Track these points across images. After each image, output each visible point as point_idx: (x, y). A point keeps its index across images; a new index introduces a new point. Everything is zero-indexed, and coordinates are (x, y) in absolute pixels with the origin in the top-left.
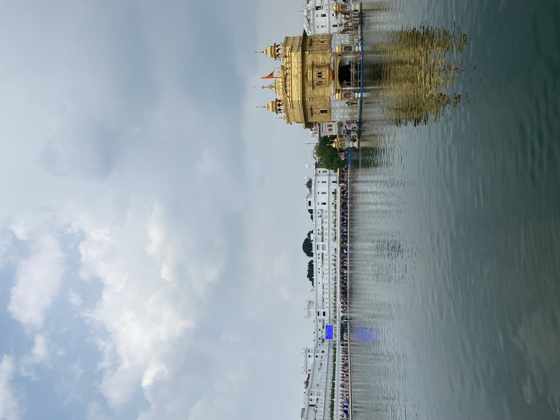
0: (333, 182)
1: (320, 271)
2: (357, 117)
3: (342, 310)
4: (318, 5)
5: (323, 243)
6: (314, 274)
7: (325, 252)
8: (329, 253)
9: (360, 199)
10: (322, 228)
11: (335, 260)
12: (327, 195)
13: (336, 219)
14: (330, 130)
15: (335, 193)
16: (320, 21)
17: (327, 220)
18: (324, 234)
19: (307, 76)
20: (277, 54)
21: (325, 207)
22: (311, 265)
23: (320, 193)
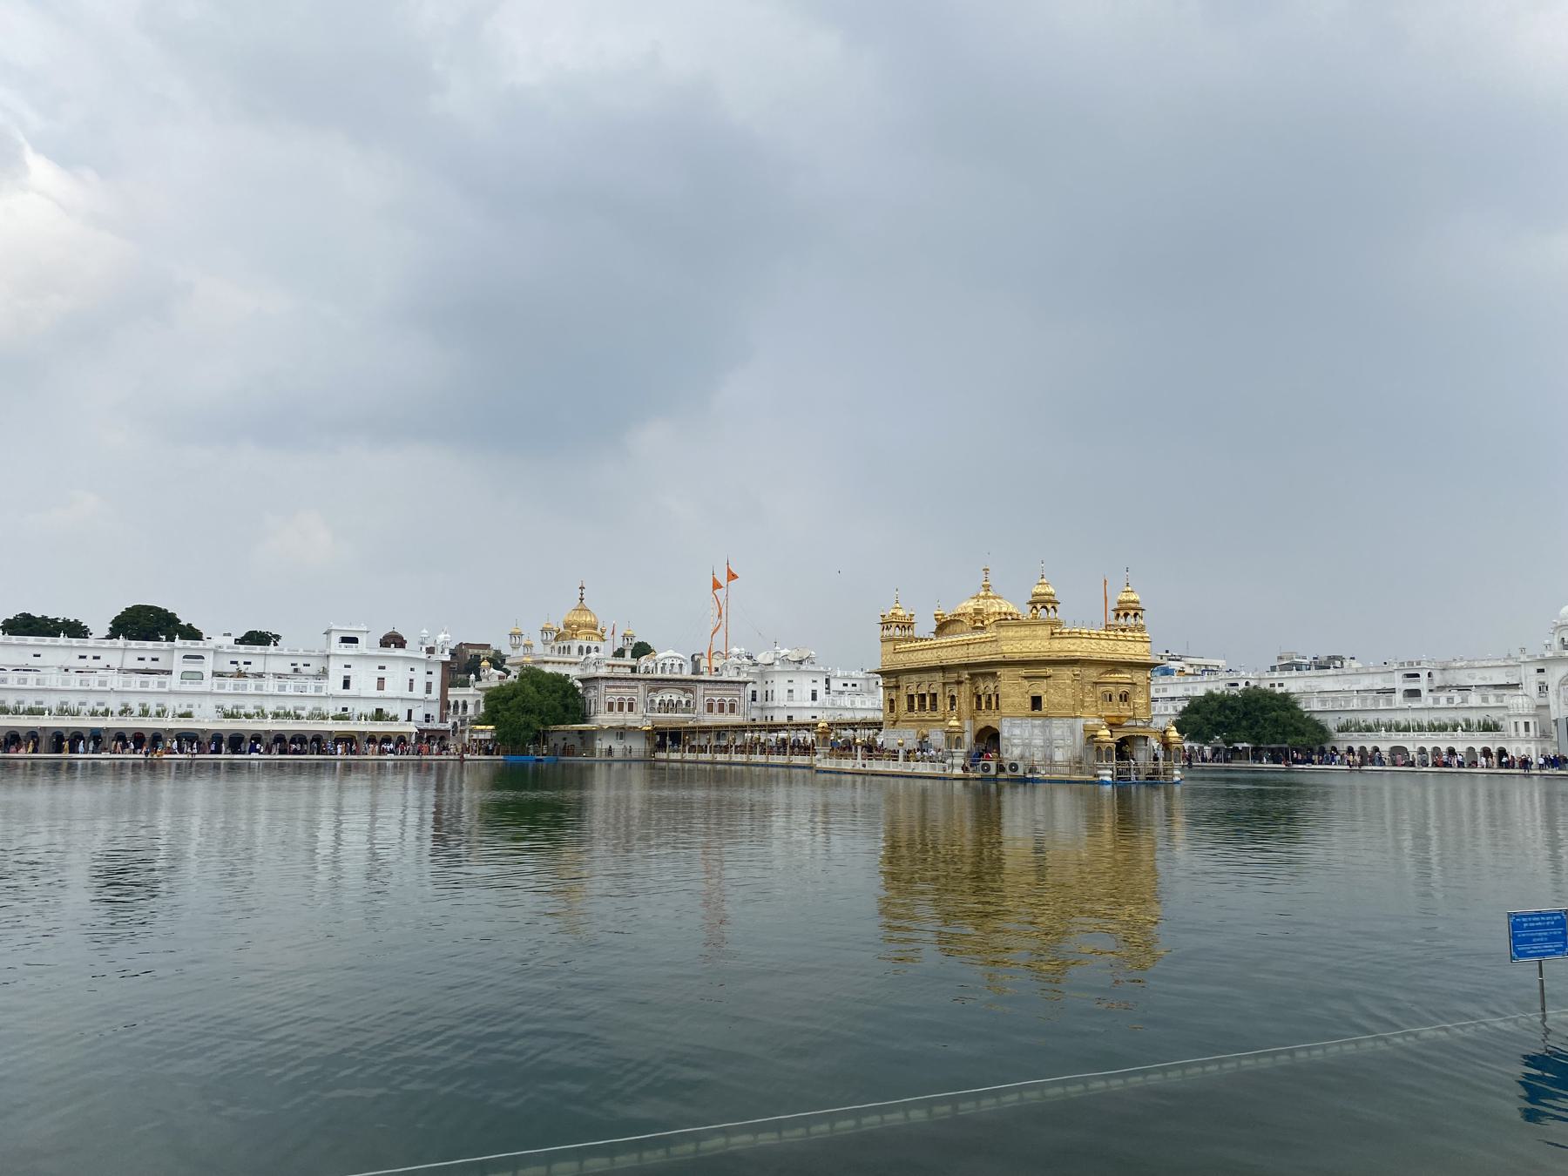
0: (410, 712)
1: (89, 662)
2: (1042, 773)
3: (1429, 749)
4: (832, 682)
5: (208, 674)
6: (74, 641)
7: (174, 682)
8: (171, 692)
9: (357, 792)
10: (260, 675)
11: (145, 713)
12: (375, 693)
13: (298, 717)
14: (611, 707)
15: (379, 715)
16: (804, 686)
17: (289, 691)
18: (241, 681)
19: (1115, 671)
21: (334, 685)
22: (76, 630)
23: (381, 674)
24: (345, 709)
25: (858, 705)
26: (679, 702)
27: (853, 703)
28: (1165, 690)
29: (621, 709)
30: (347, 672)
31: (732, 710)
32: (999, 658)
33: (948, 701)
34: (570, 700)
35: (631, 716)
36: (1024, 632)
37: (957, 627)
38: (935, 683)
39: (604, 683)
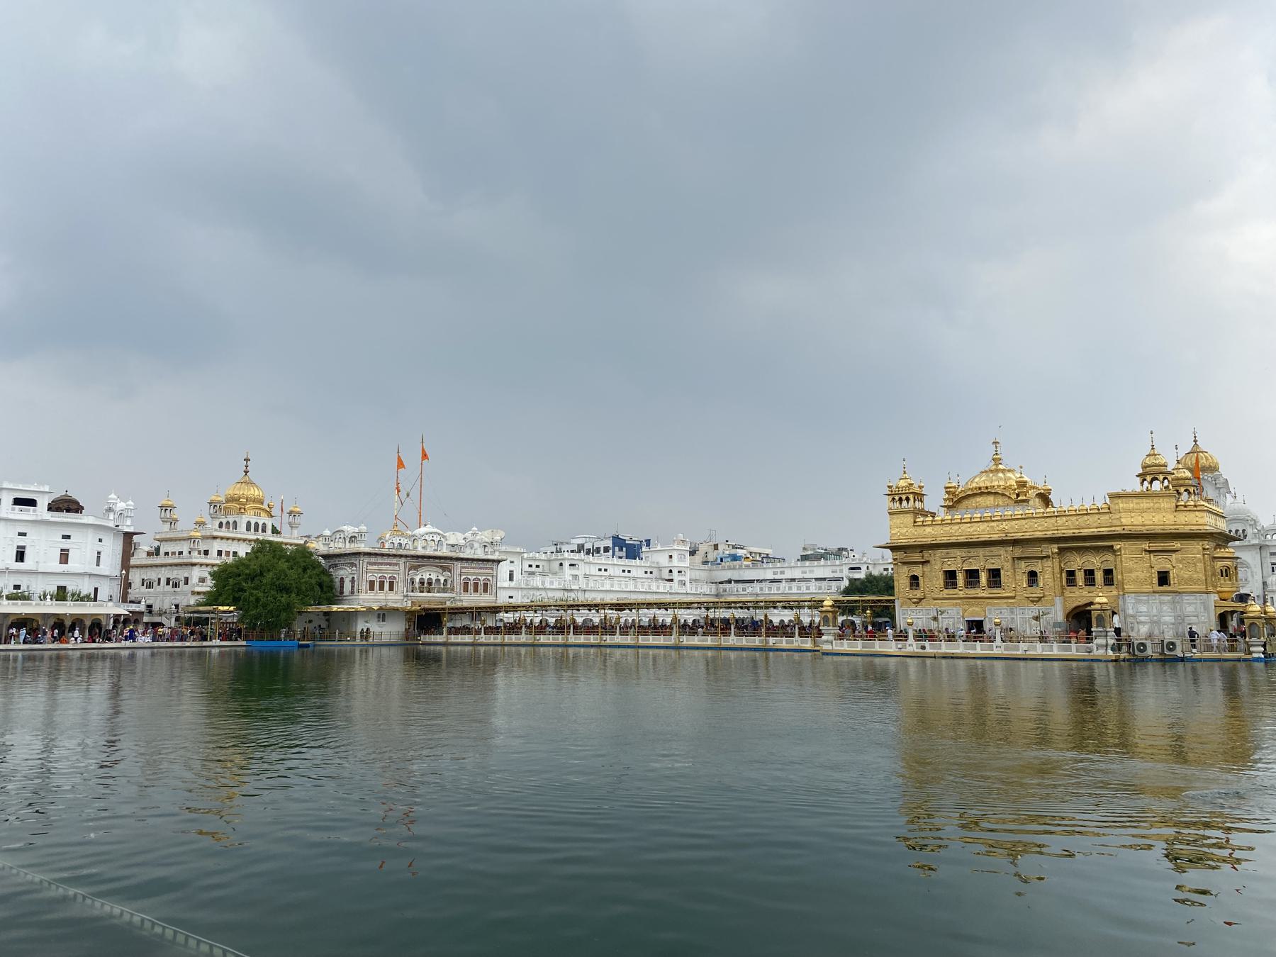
0: (96, 589)
19: (1218, 546)
20: (1182, 490)
23: (65, 544)
24: (17, 587)
25: (548, 585)
26: (438, 580)
27: (543, 583)
28: (782, 573)
29: (382, 588)
30: (21, 541)
31: (485, 590)
32: (1119, 530)
33: (1025, 578)
34: (325, 578)
35: (392, 596)
36: (1145, 504)
37: (990, 500)
38: (1001, 559)
39: (366, 559)
